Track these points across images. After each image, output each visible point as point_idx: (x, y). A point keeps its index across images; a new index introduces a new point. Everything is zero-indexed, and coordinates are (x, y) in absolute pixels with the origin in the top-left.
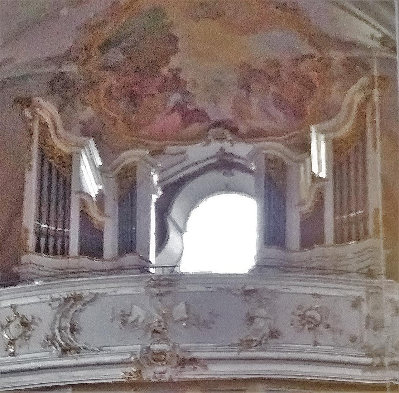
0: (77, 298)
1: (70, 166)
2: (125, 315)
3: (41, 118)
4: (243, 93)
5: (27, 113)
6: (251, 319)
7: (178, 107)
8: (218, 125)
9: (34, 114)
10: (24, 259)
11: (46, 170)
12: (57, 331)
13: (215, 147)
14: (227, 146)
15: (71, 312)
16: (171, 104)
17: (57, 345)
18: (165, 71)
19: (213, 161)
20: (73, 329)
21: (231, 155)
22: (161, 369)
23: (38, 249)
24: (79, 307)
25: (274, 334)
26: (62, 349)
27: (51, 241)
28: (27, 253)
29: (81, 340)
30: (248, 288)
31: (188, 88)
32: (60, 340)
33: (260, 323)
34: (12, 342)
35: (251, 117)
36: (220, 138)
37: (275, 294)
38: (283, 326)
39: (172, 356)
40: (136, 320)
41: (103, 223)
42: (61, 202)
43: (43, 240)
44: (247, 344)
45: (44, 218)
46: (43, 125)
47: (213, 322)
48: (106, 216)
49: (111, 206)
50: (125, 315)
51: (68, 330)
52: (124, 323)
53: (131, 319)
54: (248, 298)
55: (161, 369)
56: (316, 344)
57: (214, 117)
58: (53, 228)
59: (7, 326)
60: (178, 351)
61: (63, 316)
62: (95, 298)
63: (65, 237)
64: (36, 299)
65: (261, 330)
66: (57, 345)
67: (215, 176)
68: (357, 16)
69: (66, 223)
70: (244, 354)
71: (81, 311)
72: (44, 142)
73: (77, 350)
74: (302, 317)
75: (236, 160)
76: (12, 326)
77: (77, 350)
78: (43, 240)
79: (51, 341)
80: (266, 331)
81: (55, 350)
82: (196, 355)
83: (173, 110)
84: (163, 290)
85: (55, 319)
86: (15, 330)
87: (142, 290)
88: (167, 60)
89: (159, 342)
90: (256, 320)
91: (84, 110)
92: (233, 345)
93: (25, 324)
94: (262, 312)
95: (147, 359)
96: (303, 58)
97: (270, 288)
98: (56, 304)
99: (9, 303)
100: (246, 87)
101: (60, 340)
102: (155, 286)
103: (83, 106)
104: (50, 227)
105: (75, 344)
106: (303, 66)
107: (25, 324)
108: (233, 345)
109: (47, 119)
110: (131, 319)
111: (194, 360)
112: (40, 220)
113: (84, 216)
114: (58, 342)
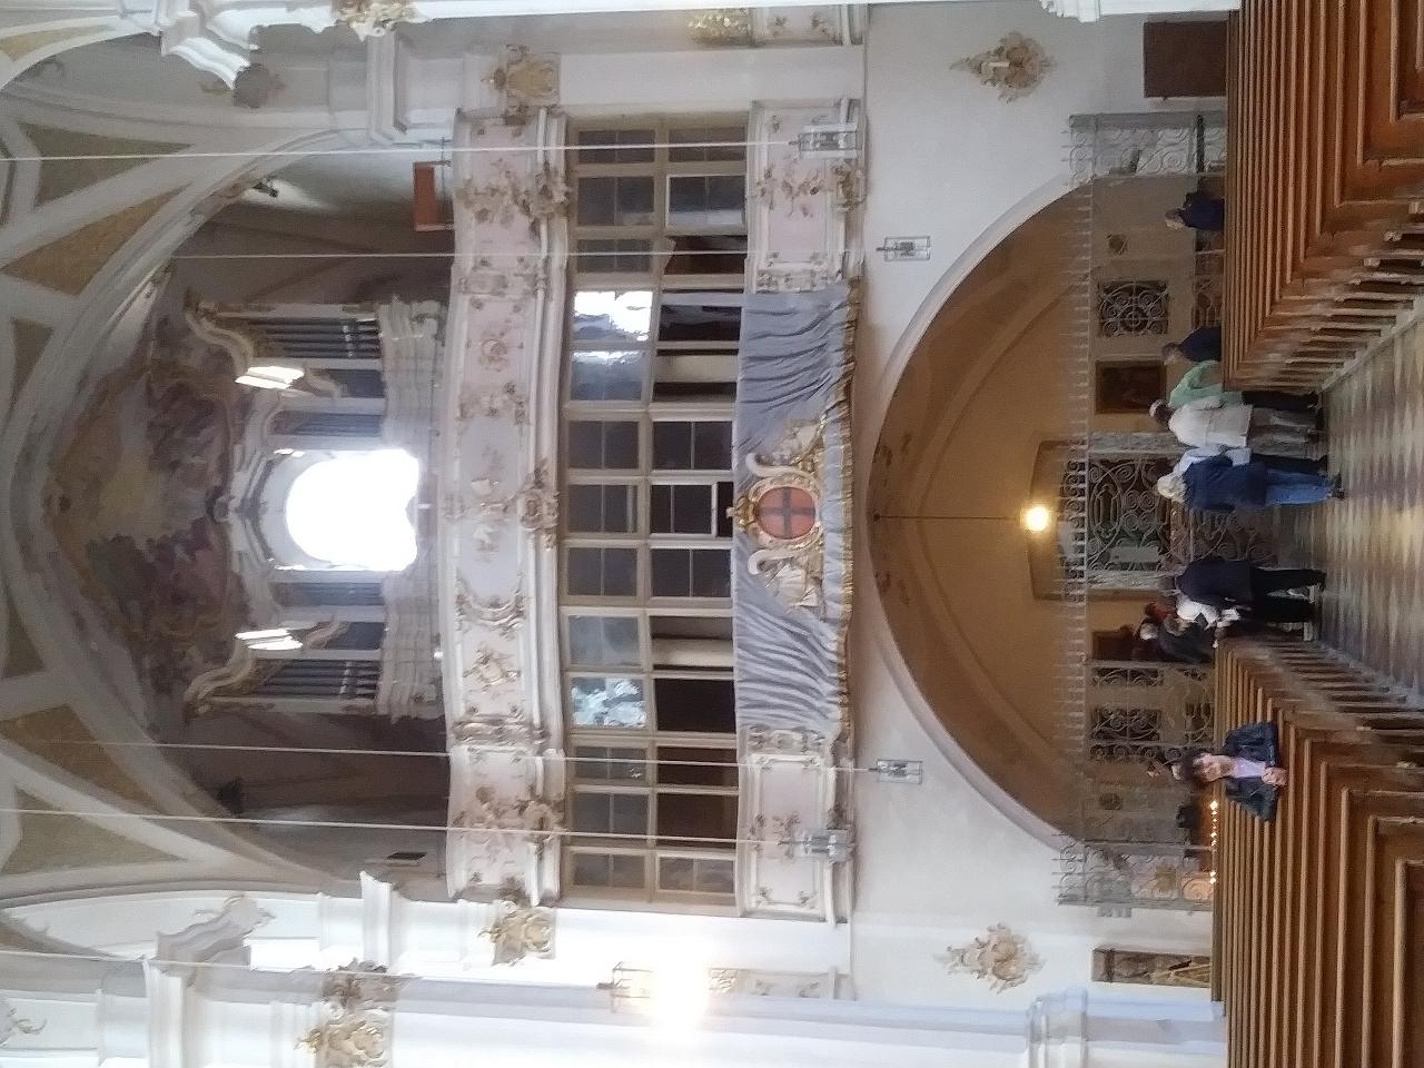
0: (461, 600)
1: (269, 661)
2: (483, 547)
3: (208, 695)
4: (179, 471)
5: (202, 710)
6: (493, 412)
7: (190, 551)
8: (210, 511)
9: (204, 701)
10: (382, 711)
11: (272, 689)
12: (497, 623)
13: (232, 518)
14: (234, 504)
15: (476, 607)
16: (187, 558)
17: (512, 622)
18: (151, 559)
19: (248, 522)
20: (495, 605)
21: (243, 500)
22: (545, 507)
23: (372, 696)
24: (470, 598)
25: (510, 389)
26: (518, 616)
27: (360, 682)
28: (375, 708)
29: (509, 597)
30: (458, 414)
31: (170, 534)
32: (506, 620)
33: (498, 404)
34: (505, 675)
35: (205, 467)
36: (225, 512)
37: (465, 387)
38: (501, 379)
39: (532, 494)
40: (489, 534)
41: (342, 623)
42: (312, 672)
43: (359, 691)
44: (520, 417)
45: (333, 689)
46: (218, 692)
47: (496, 452)
48: (333, 618)
49: (322, 614)
50: (483, 547)
51: (496, 610)
52: (491, 548)
53: (488, 541)
54: (469, 415)
55: (545, 507)
56: (521, 347)
57: (200, 513)
58: (344, 682)
59: (487, 680)
60: (528, 487)
61: (480, 615)
62: (461, 580)
63: (358, 666)
64: (459, 648)
65: (505, 402)
66: (512, 622)
67: (266, 524)
68: (121, 316)
69: (340, 665)
70: (532, 419)
71: (475, 596)
72: (239, 692)
73: (519, 600)
74: (492, 359)
75: (249, 495)
76: (487, 675)
77: (519, 600)
78: (359, 691)
79: (507, 630)
80: (506, 397)
81: (518, 624)
82: (532, 469)
83: (194, 559)
84: (457, 505)
85: (482, 625)
86: (492, 672)
87: (455, 528)
88: (139, 553)
89: (515, 511)
90: (495, 406)
91: (191, 658)
92: (521, 431)
93: (486, 660)
94: (485, 400)
95: (533, 521)
96: (149, 391)
97: (458, 392)
98: (466, 624)
99: (461, 679)
100: (174, 465)
101: (506, 620)
102: (451, 513)
103: (187, 659)
104: (344, 682)
105: (512, 603)
106: (158, 394)
107: (486, 660)
108: (521, 431)
109: (210, 687)
110: (488, 541)
111: (537, 471)
112: (336, 694)
113: (332, 643)
114: (508, 621)
